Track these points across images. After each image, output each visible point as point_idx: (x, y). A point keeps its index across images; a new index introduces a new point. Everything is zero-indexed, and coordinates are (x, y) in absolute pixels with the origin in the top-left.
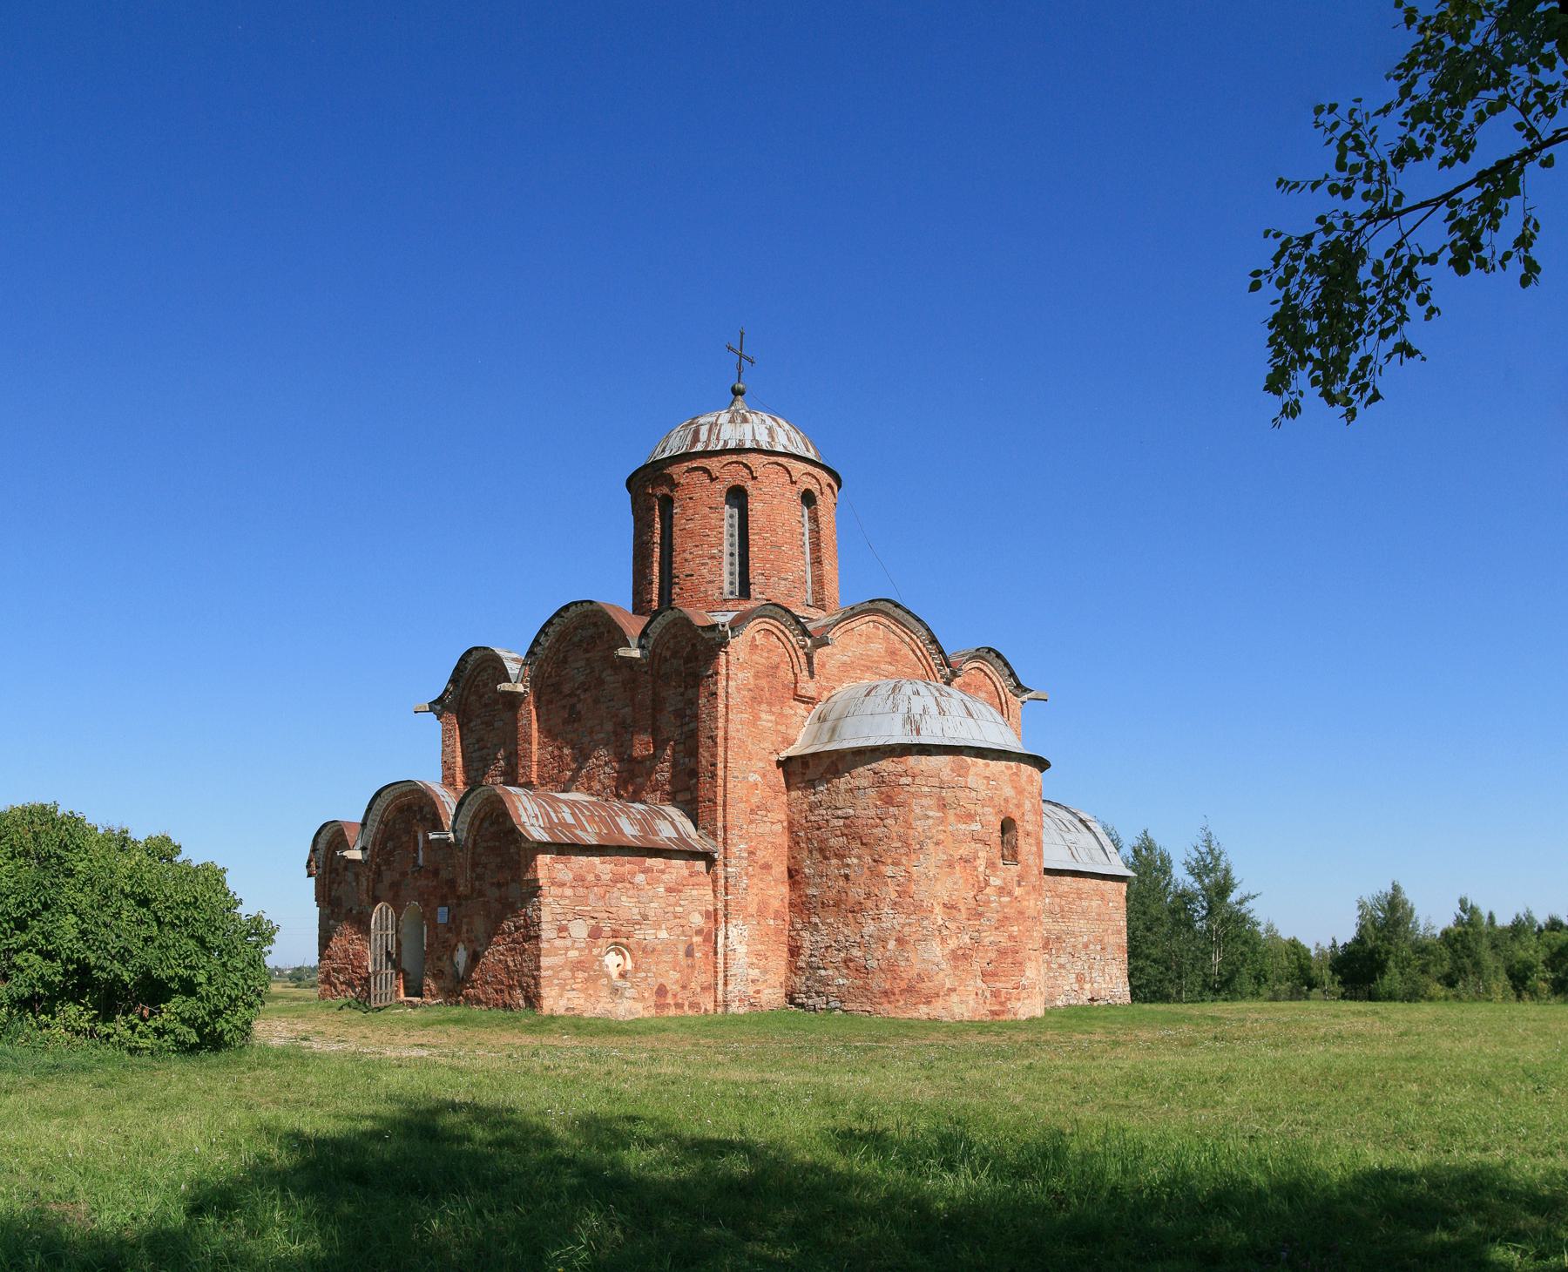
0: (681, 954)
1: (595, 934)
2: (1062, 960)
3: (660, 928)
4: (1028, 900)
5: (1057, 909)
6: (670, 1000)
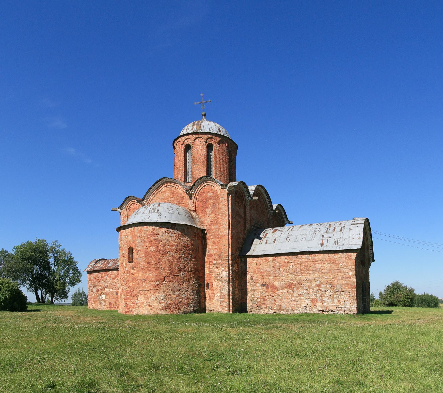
0: (115, 294)
1: (97, 290)
2: (301, 293)
3: (110, 288)
4: (139, 274)
5: (298, 270)
6: (112, 306)
